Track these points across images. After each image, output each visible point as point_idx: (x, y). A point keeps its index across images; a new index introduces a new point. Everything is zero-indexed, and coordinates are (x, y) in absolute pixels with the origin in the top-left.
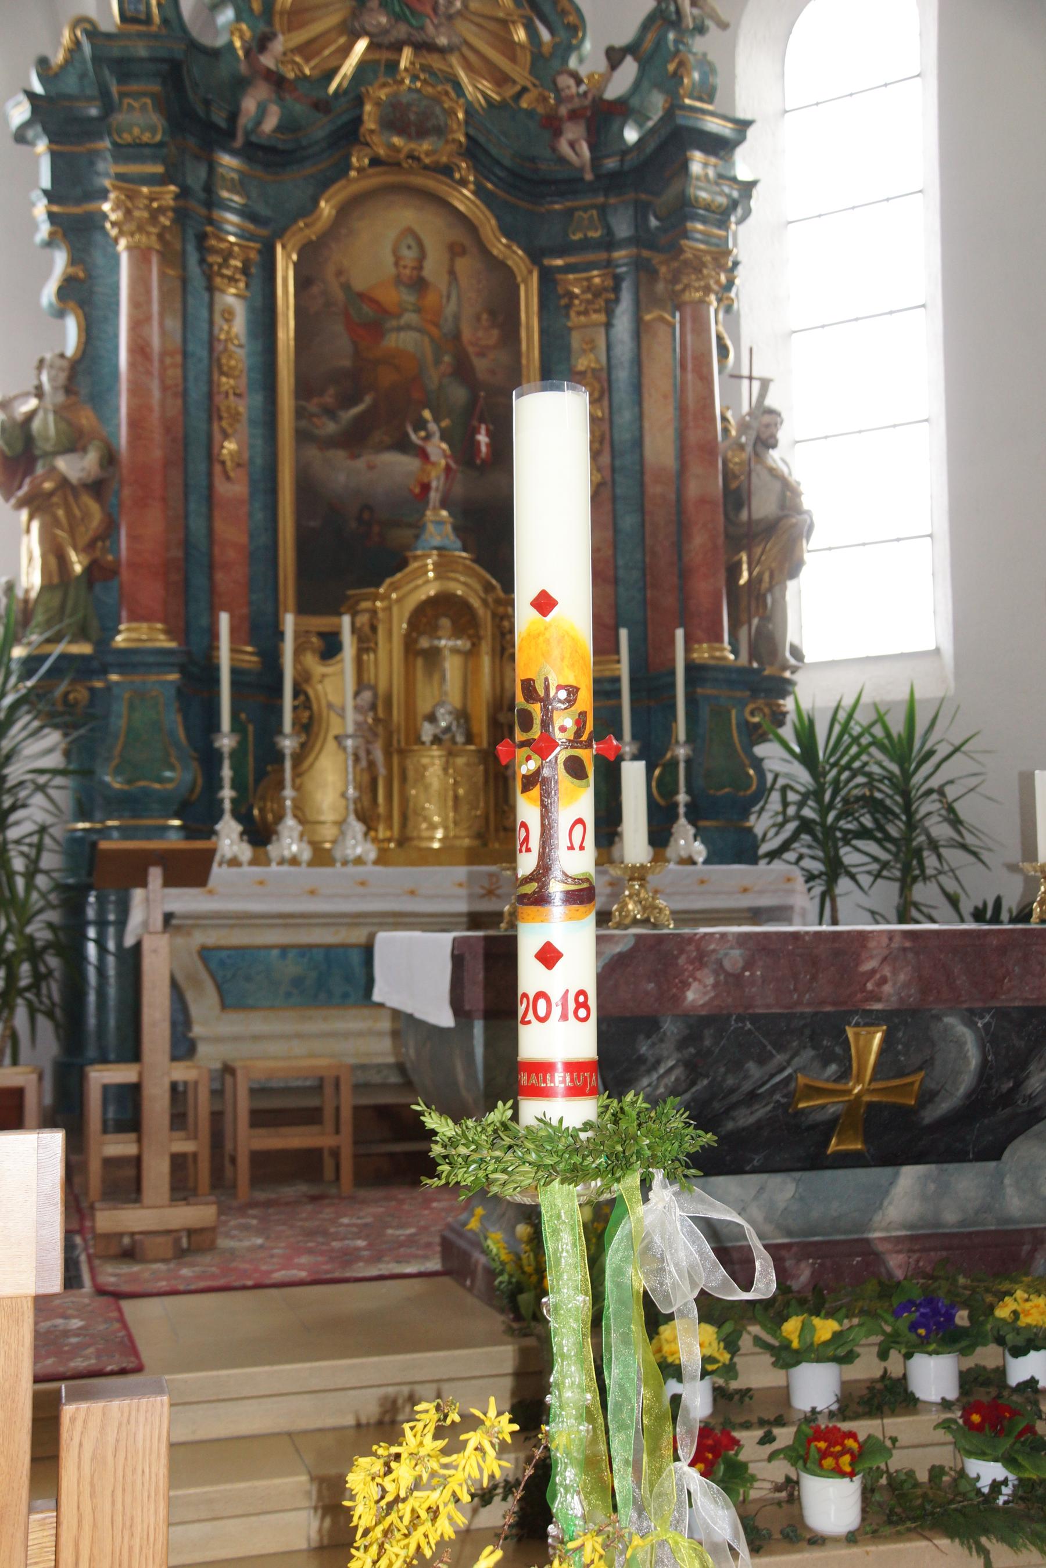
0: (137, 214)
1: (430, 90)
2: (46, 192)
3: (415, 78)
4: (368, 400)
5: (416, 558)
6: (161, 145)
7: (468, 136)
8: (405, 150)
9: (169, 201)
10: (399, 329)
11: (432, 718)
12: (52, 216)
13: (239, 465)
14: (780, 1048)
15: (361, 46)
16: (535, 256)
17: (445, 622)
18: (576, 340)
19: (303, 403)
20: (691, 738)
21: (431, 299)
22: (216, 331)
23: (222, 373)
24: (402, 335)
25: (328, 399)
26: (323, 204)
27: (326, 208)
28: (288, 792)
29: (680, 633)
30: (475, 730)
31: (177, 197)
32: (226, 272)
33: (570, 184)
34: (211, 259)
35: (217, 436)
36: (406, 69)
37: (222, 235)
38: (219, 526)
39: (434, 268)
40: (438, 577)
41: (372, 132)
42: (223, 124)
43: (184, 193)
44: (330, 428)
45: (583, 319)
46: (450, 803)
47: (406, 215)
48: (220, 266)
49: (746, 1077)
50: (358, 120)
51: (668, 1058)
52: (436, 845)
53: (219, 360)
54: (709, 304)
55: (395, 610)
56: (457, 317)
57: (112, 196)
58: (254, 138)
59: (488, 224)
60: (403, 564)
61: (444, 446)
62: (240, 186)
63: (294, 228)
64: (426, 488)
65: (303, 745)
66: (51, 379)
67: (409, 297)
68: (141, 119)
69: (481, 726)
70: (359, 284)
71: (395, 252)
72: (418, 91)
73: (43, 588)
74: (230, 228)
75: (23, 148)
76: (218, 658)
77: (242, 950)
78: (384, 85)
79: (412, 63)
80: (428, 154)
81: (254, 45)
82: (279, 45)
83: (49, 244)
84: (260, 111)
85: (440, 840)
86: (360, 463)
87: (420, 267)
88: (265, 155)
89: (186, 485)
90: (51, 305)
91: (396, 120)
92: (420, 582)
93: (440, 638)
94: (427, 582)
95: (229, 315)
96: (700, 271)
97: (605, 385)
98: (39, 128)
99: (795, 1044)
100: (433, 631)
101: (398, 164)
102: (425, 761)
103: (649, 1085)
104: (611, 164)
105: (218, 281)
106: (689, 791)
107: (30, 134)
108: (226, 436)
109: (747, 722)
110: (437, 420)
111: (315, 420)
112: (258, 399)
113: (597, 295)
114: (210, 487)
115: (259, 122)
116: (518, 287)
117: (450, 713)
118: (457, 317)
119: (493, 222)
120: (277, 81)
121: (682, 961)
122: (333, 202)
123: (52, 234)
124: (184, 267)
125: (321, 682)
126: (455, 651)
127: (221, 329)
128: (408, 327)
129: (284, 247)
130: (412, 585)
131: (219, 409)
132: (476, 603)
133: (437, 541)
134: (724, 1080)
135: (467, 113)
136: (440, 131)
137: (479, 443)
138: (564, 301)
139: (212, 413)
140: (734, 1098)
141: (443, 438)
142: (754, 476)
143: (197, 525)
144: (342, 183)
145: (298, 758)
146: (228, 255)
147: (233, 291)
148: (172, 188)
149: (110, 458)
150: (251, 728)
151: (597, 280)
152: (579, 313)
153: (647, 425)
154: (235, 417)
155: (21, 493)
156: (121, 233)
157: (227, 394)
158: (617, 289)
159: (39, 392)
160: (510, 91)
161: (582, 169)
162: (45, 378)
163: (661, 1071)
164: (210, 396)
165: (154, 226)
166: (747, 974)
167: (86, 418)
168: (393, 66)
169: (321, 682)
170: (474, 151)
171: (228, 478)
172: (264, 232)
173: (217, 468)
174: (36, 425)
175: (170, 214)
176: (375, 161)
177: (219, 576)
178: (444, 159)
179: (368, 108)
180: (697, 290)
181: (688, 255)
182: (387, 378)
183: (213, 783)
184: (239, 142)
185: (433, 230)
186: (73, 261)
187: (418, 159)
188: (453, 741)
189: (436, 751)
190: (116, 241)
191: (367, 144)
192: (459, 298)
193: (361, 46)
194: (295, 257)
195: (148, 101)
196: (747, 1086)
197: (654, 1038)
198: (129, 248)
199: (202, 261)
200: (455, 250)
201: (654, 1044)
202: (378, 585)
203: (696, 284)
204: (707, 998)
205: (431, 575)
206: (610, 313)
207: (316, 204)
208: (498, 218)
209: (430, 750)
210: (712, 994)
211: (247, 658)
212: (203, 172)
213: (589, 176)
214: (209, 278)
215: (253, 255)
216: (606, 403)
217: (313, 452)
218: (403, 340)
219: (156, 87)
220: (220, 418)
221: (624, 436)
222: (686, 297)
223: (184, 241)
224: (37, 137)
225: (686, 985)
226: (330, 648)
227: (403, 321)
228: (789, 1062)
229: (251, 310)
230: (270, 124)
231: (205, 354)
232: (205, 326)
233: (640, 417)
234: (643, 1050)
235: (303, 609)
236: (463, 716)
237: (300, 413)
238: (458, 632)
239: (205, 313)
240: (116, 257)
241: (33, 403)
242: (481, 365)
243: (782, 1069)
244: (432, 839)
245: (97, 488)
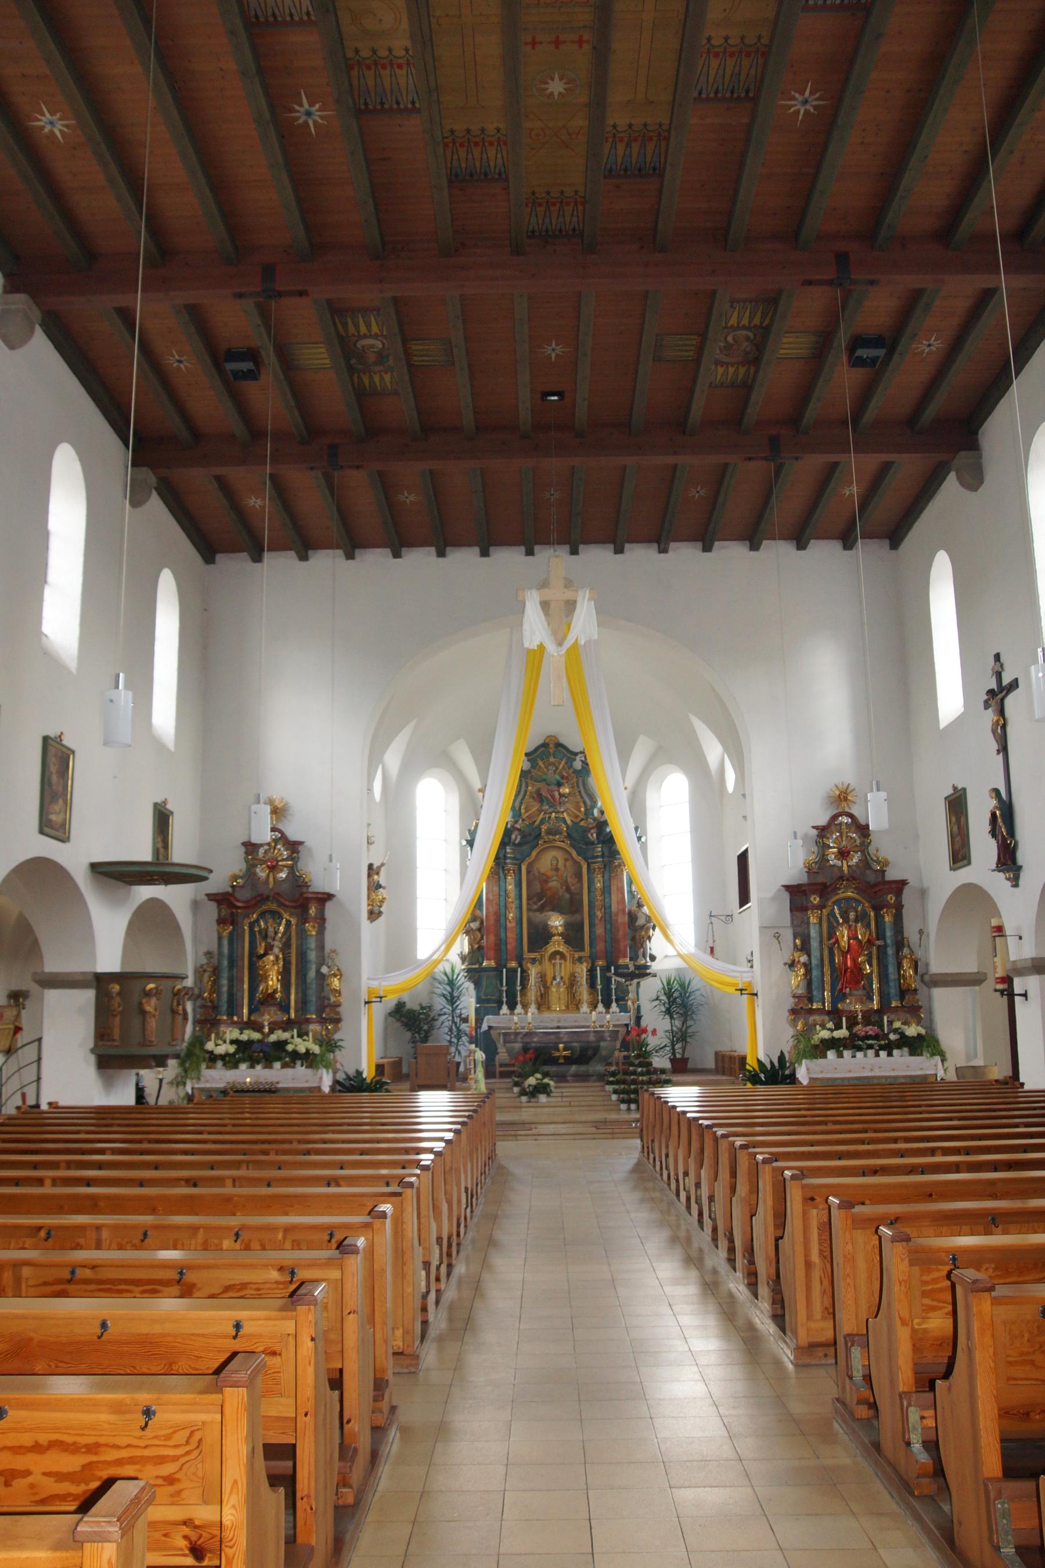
11: (554, 978)
16: (586, 860)
17: (558, 957)
21: (560, 873)
25: (535, 899)
27: (534, 854)
33: (592, 843)
39: (561, 865)
44: (536, 907)
47: (553, 853)
67: (555, 873)
69: (567, 982)
70: (542, 871)
84: (516, 837)
104: (601, 838)
112: (518, 902)
136: (561, 833)
139: (506, 908)
143: (503, 935)
146: (509, 870)
149: (482, 923)
167: (478, 912)
170: (569, 836)
177: (509, 946)
182: (549, 893)
183: (501, 996)
185: (560, 855)
192: (568, 873)
200: (566, 860)
217: (531, 913)
218: (553, 884)
221: (607, 905)
230: (518, 840)
237: (528, 904)
242: (572, 888)
245: (479, 930)
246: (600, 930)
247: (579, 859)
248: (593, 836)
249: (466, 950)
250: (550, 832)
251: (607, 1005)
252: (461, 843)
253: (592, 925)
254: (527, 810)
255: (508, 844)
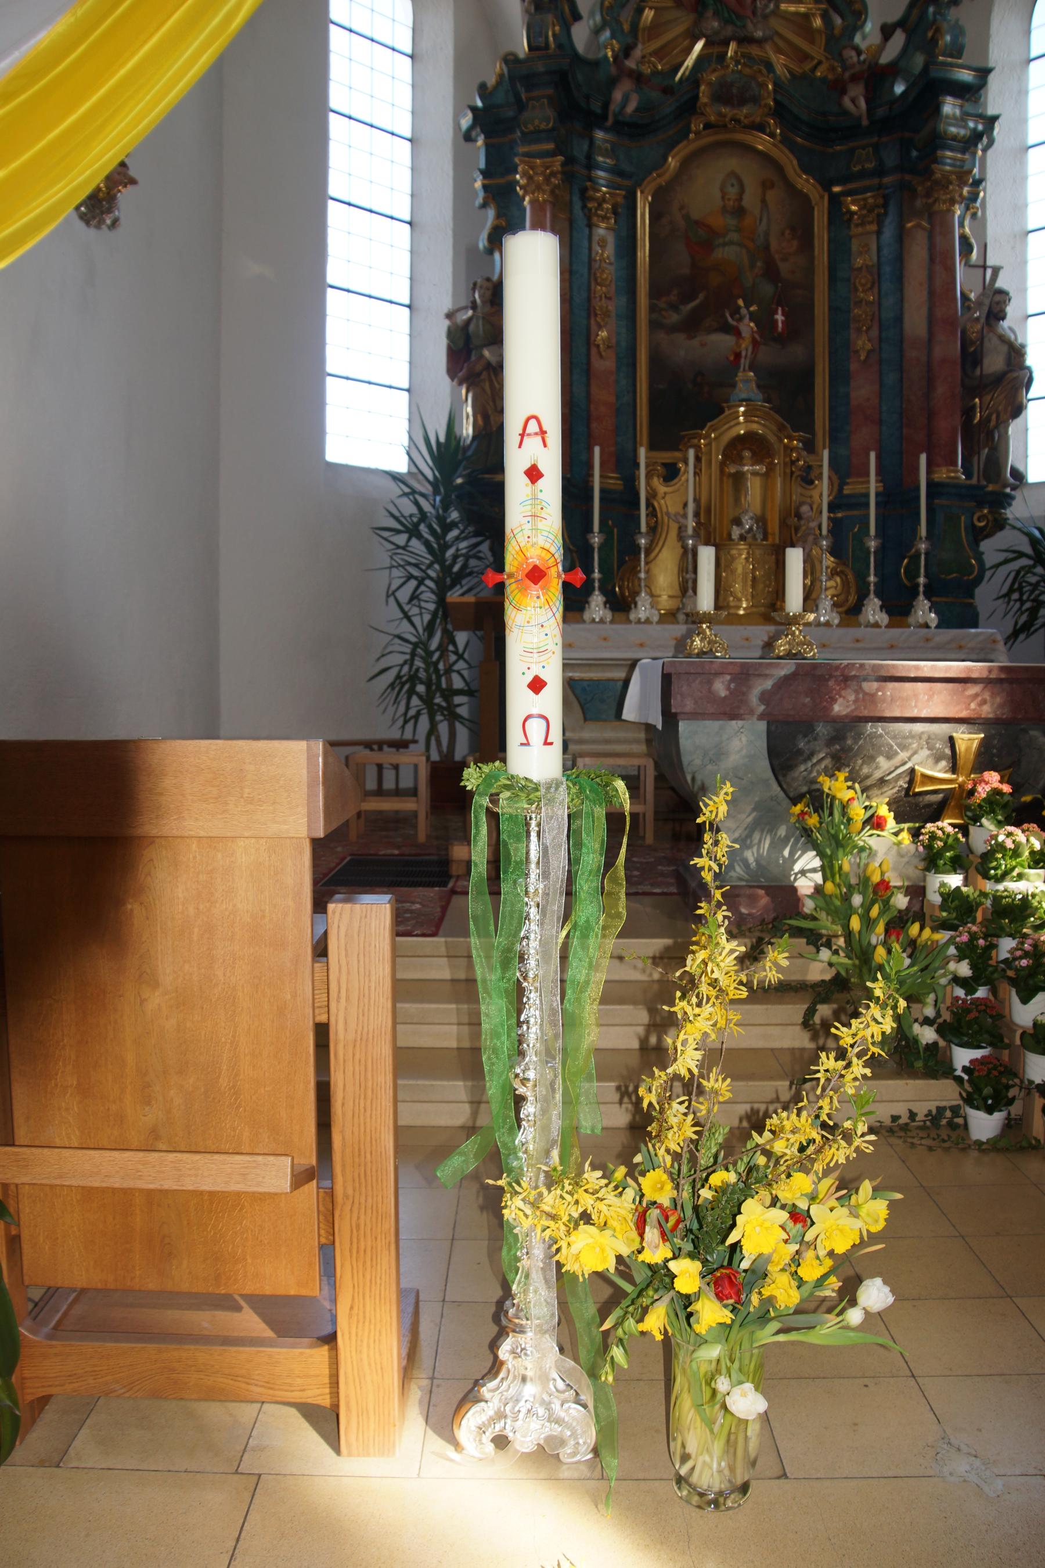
0: (536, 178)
1: (747, 71)
2: (482, 172)
3: (737, 63)
4: (701, 296)
5: (729, 408)
6: (553, 129)
7: (775, 100)
8: (729, 116)
9: (557, 167)
10: (725, 244)
11: (738, 522)
12: (485, 187)
13: (609, 347)
14: (904, 747)
15: (699, 46)
18: (855, 245)
19: (655, 301)
20: (930, 536)
22: (593, 255)
23: (598, 284)
24: (727, 248)
25: (673, 297)
26: (670, 159)
27: (672, 162)
28: (642, 575)
29: (923, 457)
30: (770, 530)
31: (563, 165)
32: (599, 212)
33: (851, 130)
34: (590, 205)
35: (594, 327)
36: (731, 58)
37: (597, 187)
38: (594, 390)
39: (751, 200)
40: (746, 421)
41: (706, 105)
42: (599, 111)
43: (570, 161)
44: (674, 318)
45: (860, 230)
46: (750, 583)
47: (732, 163)
48: (597, 209)
49: (877, 768)
50: (696, 98)
51: (819, 752)
52: (741, 612)
53: (595, 274)
54: (954, 213)
55: (714, 445)
56: (767, 234)
57: (520, 169)
58: (620, 118)
59: (790, 163)
60: (722, 411)
61: (752, 324)
62: (612, 153)
63: (648, 179)
64: (738, 356)
65: (652, 541)
66: (480, 296)
67: (732, 222)
68: (541, 115)
70: (696, 215)
71: (722, 190)
72: (740, 72)
73: (474, 438)
74: (602, 182)
75: (470, 145)
76: (593, 481)
77: (598, 682)
78: (715, 70)
79: (736, 53)
80: (746, 117)
81: (621, 55)
82: (638, 52)
83: (484, 206)
84: (626, 100)
85: (745, 609)
86: (695, 342)
87: (740, 199)
88: (631, 130)
89: (571, 363)
90: (484, 247)
91: (723, 95)
92: (732, 423)
93: (744, 465)
94: (739, 423)
95: (603, 243)
96: (947, 188)
97: (876, 277)
98: (478, 129)
99: (914, 746)
100: (740, 460)
101: (725, 126)
102: (734, 552)
103: (805, 770)
104: (881, 112)
105: (595, 219)
106: (926, 576)
107: (474, 134)
108: (600, 327)
109: (973, 526)
110: (747, 307)
111: (664, 313)
112: (623, 300)
113: (870, 211)
114: (589, 363)
115: (624, 106)
116: (813, 208)
117: (751, 518)
118: (767, 234)
119: (795, 162)
120: (638, 78)
121: (831, 683)
122: (677, 158)
123: (485, 199)
124: (571, 212)
125: (663, 498)
126: (755, 474)
127: (597, 253)
128: (731, 243)
129: (642, 192)
130: (727, 426)
131: (595, 308)
132: (772, 438)
133: (744, 396)
134: (861, 769)
135: (775, 85)
136: (755, 100)
137: (776, 321)
138: (846, 217)
139: (590, 311)
140: (868, 782)
141: (751, 320)
142: (986, 340)
144: (685, 143)
145: (648, 552)
147: (603, 225)
148: (561, 158)
150: (615, 530)
151: (871, 201)
152: (857, 225)
153: (906, 305)
154: (606, 314)
155: (460, 374)
156: (526, 193)
157: (601, 297)
158: (885, 205)
159: (474, 306)
160: (808, 66)
161: (860, 118)
162: (477, 296)
163: (815, 761)
164: (589, 300)
165: (548, 185)
166: (880, 693)
168: (722, 56)
169: (663, 498)
170: (780, 111)
171: (601, 356)
172: (627, 183)
173: (594, 351)
174: (472, 327)
175: (559, 176)
176: (708, 126)
177: (594, 425)
178: (758, 120)
179: (703, 88)
180: (944, 202)
181: (938, 176)
184: (610, 122)
185: (751, 173)
186: (498, 216)
187: (738, 121)
188: (754, 538)
189: (742, 546)
190: (524, 200)
191: (702, 114)
193: (699, 46)
194: (650, 198)
195: (545, 101)
196: (878, 775)
197: (810, 737)
198: (531, 202)
199: (584, 207)
200: (766, 185)
201: (809, 741)
202: (702, 429)
203: (944, 197)
204: (849, 710)
205: (741, 418)
206: (880, 223)
207: (666, 159)
208: (799, 161)
209: (738, 544)
210: (853, 707)
211: (611, 481)
212: (586, 147)
213: (865, 122)
214: (589, 219)
215: (620, 200)
216: (876, 290)
218: (727, 253)
219: (550, 91)
220: (596, 315)
222: (936, 207)
223: (571, 194)
224: (477, 136)
225: (834, 700)
226: (671, 473)
227: (727, 239)
228: (909, 759)
229: (618, 238)
230: (630, 108)
231: (585, 271)
232: (587, 251)
233: (901, 300)
234: (801, 745)
235: (652, 447)
236: (761, 520)
237: (652, 309)
238: (757, 459)
239: (586, 243)
240: (525, 210)
241: (470, 313)
242: (784, 268)
243: (904, 763)
244: (739, 607)
246: (862, 391)
247: (805, 183)
248: (856, 102)
249: (467, 430)
250: (723, 95)
251: (898, 609)
252: (457, 125)
253: (839, 377)
254: (654, 30)
255: (597, 120)
